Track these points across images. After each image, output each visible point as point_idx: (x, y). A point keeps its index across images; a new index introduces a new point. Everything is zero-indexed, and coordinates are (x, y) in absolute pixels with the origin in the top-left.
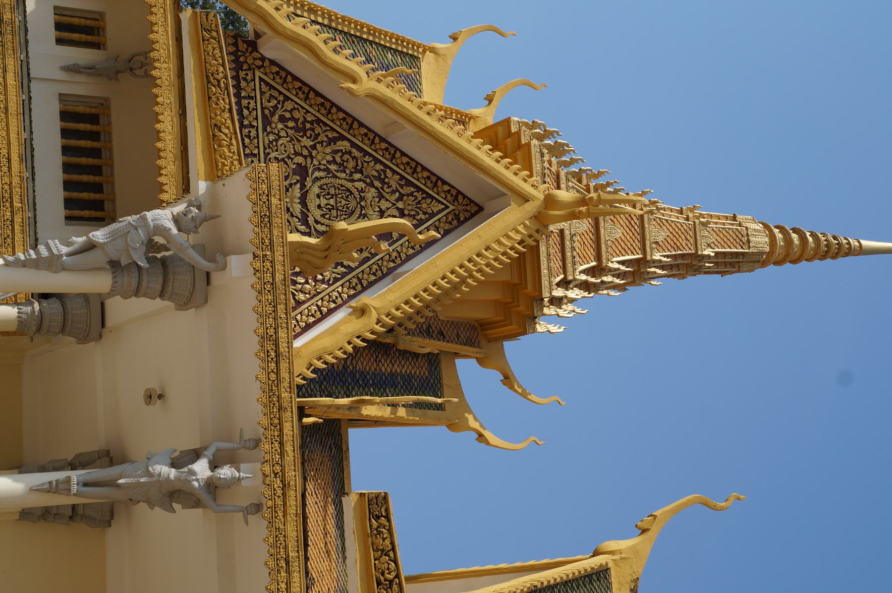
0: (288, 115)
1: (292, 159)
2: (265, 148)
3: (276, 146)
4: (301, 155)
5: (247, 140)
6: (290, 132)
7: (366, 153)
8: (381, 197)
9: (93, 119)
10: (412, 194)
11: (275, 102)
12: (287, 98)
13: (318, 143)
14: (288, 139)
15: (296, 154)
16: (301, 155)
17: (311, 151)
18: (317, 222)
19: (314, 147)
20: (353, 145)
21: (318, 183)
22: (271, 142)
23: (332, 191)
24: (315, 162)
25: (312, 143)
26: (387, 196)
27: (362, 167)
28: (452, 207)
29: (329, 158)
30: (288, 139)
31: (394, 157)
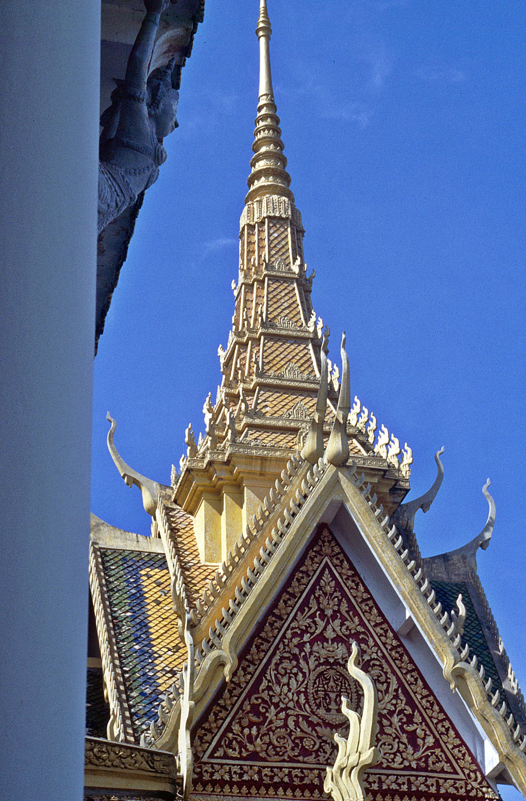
1: (291, 731)
2: (284, 761)
3: (280, 748)
4: (286, 719)
11: (234, 742)
12: (229, 729)
13: (271, 700)
14: (271, 733)
15: (286, 726)
16: (286, 719)
17: (279, 709)
19: (276, 705)
24: (291, 705)
25: (272, 707)
27: (290, 652)
30: (271, 733)
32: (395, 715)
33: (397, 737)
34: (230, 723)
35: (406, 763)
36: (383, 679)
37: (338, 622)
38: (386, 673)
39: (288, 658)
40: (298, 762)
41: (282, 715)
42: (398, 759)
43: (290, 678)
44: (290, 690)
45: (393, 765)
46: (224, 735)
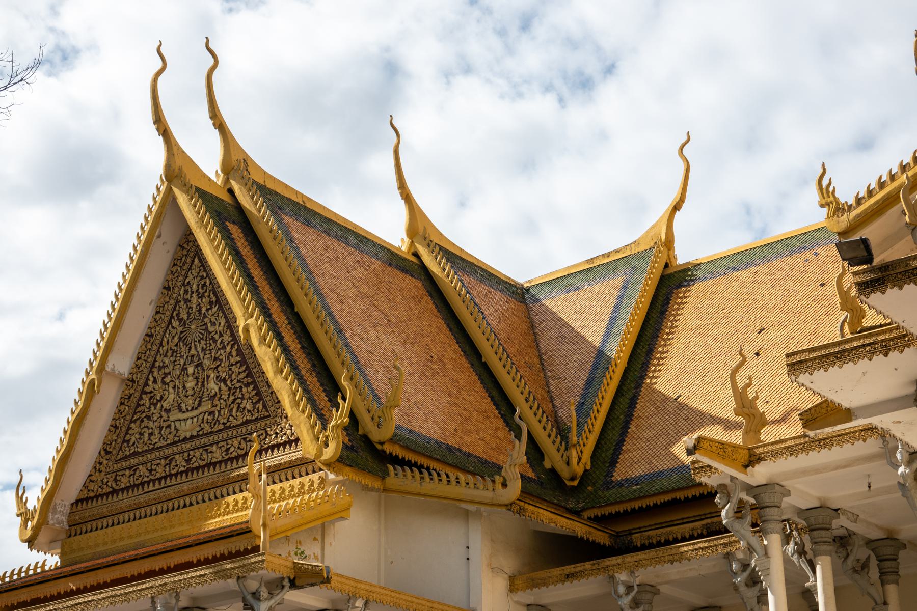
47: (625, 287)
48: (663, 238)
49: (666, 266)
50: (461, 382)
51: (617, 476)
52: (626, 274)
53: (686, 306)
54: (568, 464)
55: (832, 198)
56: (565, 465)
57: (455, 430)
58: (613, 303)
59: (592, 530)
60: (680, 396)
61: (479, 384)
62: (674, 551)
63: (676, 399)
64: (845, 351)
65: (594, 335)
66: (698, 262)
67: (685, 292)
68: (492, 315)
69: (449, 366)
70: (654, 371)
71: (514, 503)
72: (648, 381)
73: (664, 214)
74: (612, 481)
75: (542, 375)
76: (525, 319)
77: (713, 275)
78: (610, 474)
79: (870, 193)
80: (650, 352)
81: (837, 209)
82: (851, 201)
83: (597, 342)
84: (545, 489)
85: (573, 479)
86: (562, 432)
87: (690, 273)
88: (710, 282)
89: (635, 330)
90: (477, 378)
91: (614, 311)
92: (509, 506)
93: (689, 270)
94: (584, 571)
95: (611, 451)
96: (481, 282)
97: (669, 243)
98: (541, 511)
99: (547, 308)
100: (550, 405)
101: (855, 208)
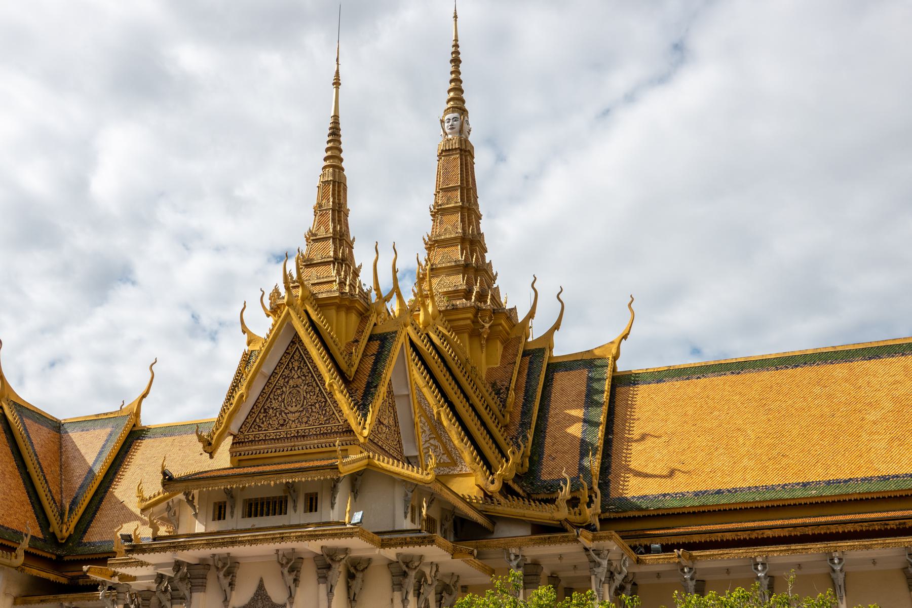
0: (261, 421)
2: (274, 430)
5: (275, 434)
6: (267, 420)
7: (275, 385)
8: (293, 378)
9: (251, 505)
10: (292, 363)
15: (276, 415)
16: (276, 413)
18: (302, 407)
20: (271, 392)
21: (287, 407)
22: (272, 427)
23: (290, 400)
26: (293, 374)
28: (297, 345)
29: (277, 401)
31: (276, 373)
32: (317, 404)
33: (318, 412)
34: (256, 418)
35: (320, 422)
36: (313, 390)
37: (299, 371)
38: (314, 388)
39: (279, 389)
40: (279, 429)
41: (275, 411)
42: (317, 422)
43: (279, 396)
44: (278, 401)
45: (315, 424)
46: (253, 424)
47: (111, 435)
48: (135, 412)
49: (134, 425)
50: (12, 485)
51: (85, 540)
52: (113, 427)
53: (138, 451)
54: (61, 531)
55: (141, 495)
56: (59, 533)
57: (3, 515)
58: (103, 443)
59: (59, 577)
60: (124, 501)
61: (22, 485)
62: (90, 596)
63: (121, 503)
64: (128, 562)
65: (90, 459)
66: (150, 427)
67: (139, 443)
68: (38, 443)
69: (7, 476)
70: (115, 485)
71: (19, 567)
72: (111, 490)
73: (136, 400)
74: (82, 542)
75: (59, 478)
76: (57, 443)
77: (155, 436)
78: (82, 538)
79: (154, 496)
80: (116, 473)
81: (143, 500)
82: (148, 497)
83: (91, 464)
84: (47, 544)
85: (62, 539)
86: (62, 515)
87: (144, 432)
88: (152, 440)
89: (110, 462)
90: (22, 481)
91: (103, 448)
92: (17, 568)
93: (144, 430)
94: (49, 599)
95: (85, 526)
96: (36, 422)
97: (137, 414)
98: (33, 570)
99: (70, 438)
100: (60, 496)
101: (148, 501)
